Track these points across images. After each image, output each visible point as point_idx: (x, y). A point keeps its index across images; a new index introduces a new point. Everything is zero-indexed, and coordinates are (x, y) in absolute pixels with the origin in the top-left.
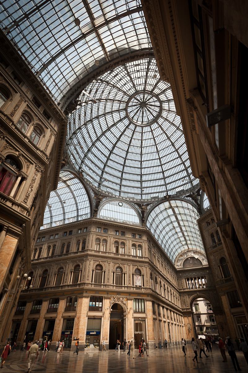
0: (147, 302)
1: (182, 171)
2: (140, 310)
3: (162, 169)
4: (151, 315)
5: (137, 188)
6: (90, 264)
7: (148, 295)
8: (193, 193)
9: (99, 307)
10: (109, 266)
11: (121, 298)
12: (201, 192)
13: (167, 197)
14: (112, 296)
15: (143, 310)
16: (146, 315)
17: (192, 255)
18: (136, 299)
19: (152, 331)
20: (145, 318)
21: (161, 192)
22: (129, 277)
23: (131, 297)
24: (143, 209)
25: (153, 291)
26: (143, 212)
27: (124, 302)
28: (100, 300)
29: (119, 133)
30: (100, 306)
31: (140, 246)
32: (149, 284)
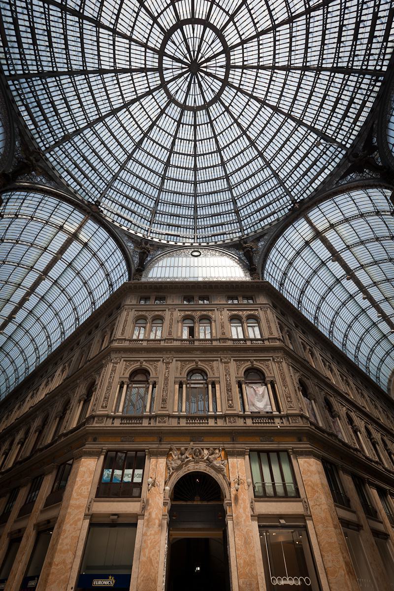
2: (280, 490)
4: (325, 507)
6: (114, 371)
7: (298, 435)
9: (132, 484)
10: (167, 368)
11: (206, 452)
13: (297, 205)
14: (174, 446)
15: (291, 488)
16: (307, 508)
18: (259, 452)
19: (343, 572)
20: (302, 518)
22: (229, 390)
23: (239, 447)
24: (251, 251)
25: (311, 423)
27: (217, 463)
28: (138, 462)
29: (168, 139)
30: (137, 480)
31: (256, 319)
32: (297, 405)
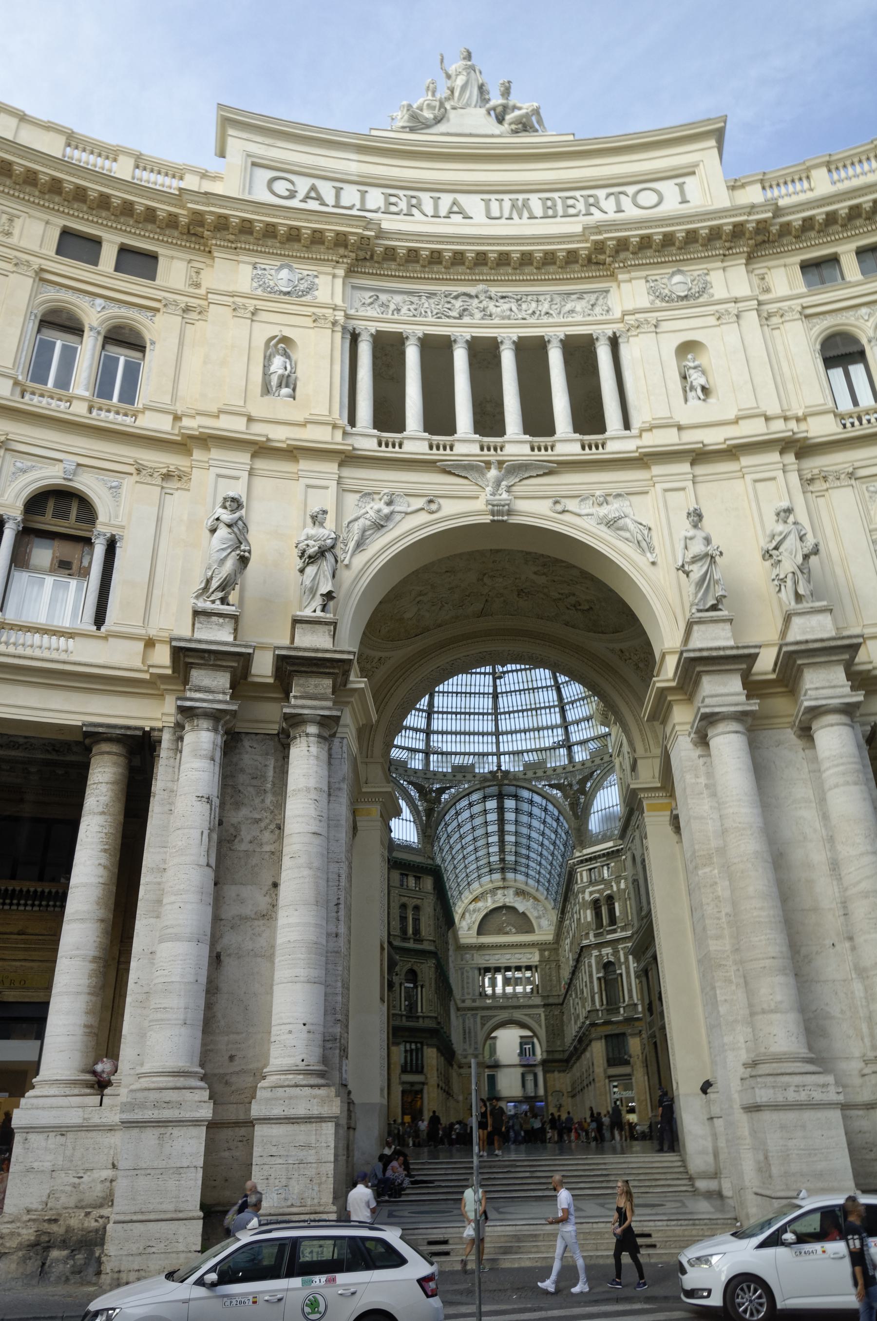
0: (430, 1050)
1: (550, 707)
3: (495, 687)
5: (416, 730)
8: (570, 785)
12: (589, 785)
13: (499, 774)
17: (508, 898)
20: (423, 1084)
21: (484, 754)
26: (429, 812)
